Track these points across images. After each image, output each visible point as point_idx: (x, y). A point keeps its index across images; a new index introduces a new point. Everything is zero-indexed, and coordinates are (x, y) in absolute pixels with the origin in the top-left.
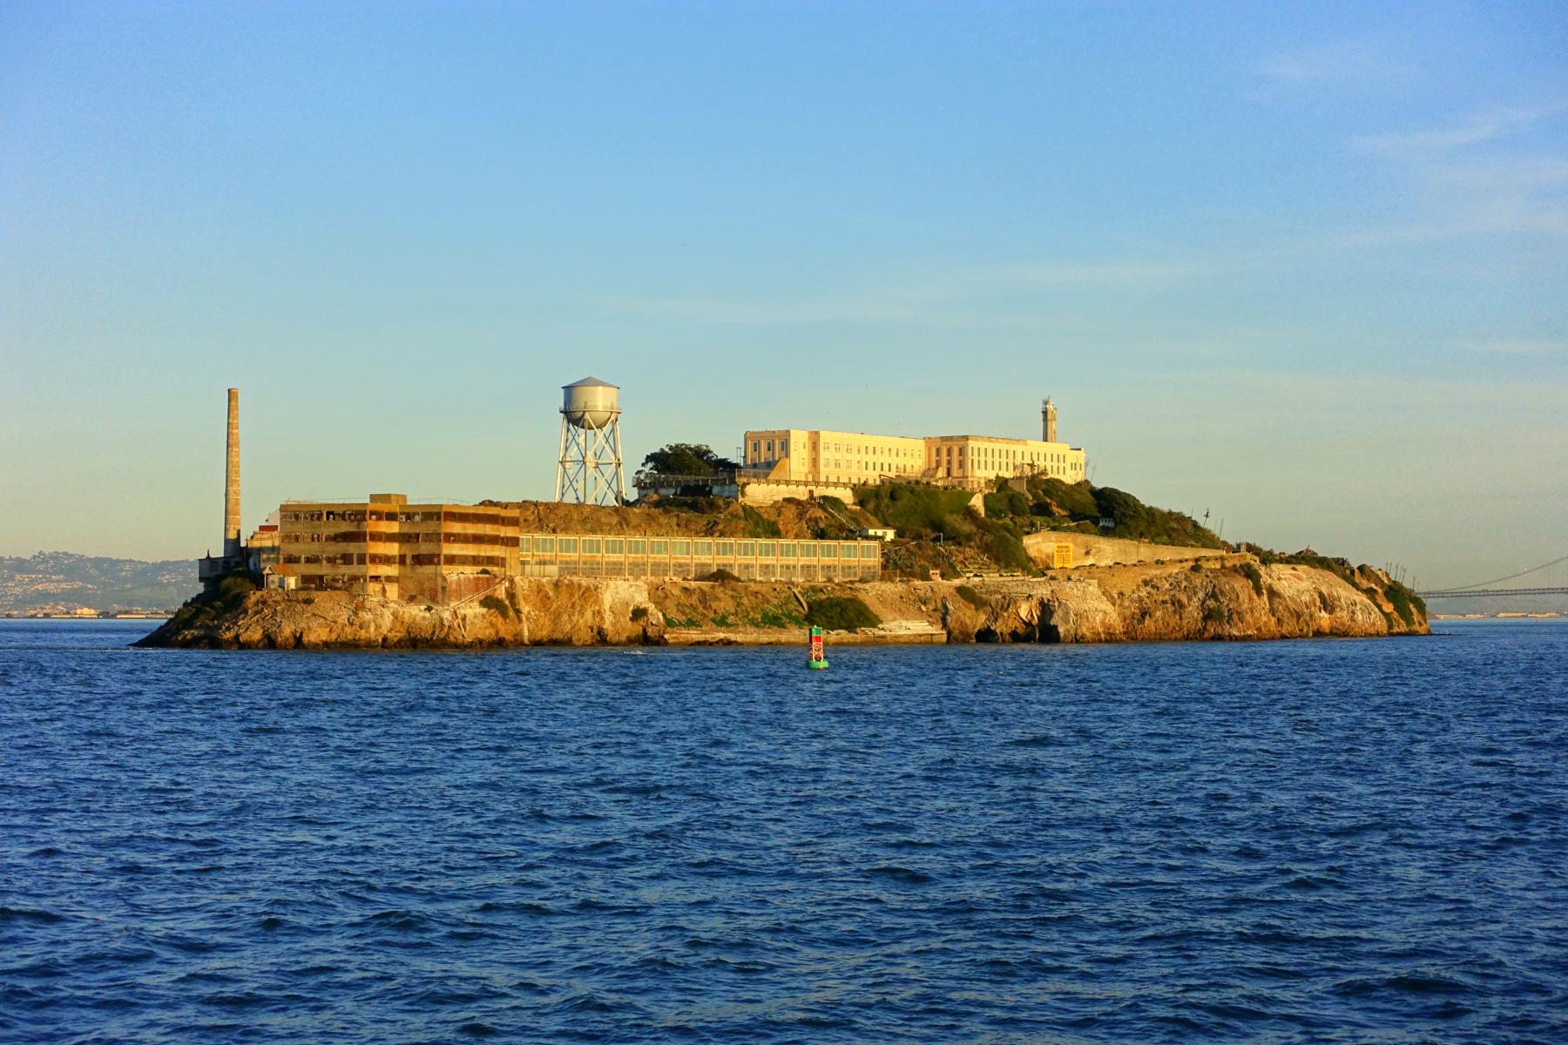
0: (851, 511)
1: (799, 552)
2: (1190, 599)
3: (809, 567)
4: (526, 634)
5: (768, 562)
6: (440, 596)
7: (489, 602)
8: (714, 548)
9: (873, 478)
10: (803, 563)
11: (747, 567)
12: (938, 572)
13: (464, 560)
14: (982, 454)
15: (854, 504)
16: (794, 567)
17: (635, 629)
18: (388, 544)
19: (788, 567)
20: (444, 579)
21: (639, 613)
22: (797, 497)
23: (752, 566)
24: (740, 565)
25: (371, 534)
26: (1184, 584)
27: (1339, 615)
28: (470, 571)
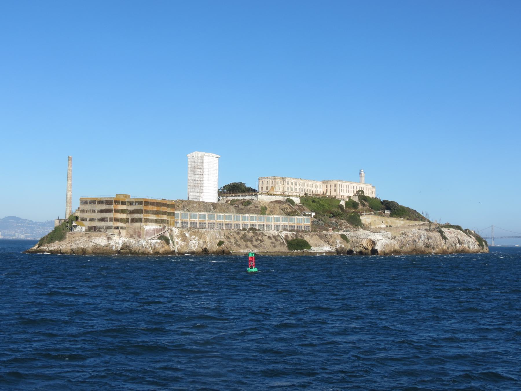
0: (298, 206)
1: (281, 220)
2: (419, 240)
5: (269, 224)
7: (162, 237)
8: (249, 218)
9: (310, 194)
10: (282, 224)
12: (332, 229)
13: (152, 221)
14: (343, 187)
15: (300, 203)
18: (121, 214)
25: (115, 210)
26: (417, 234)
27: (464, 246)
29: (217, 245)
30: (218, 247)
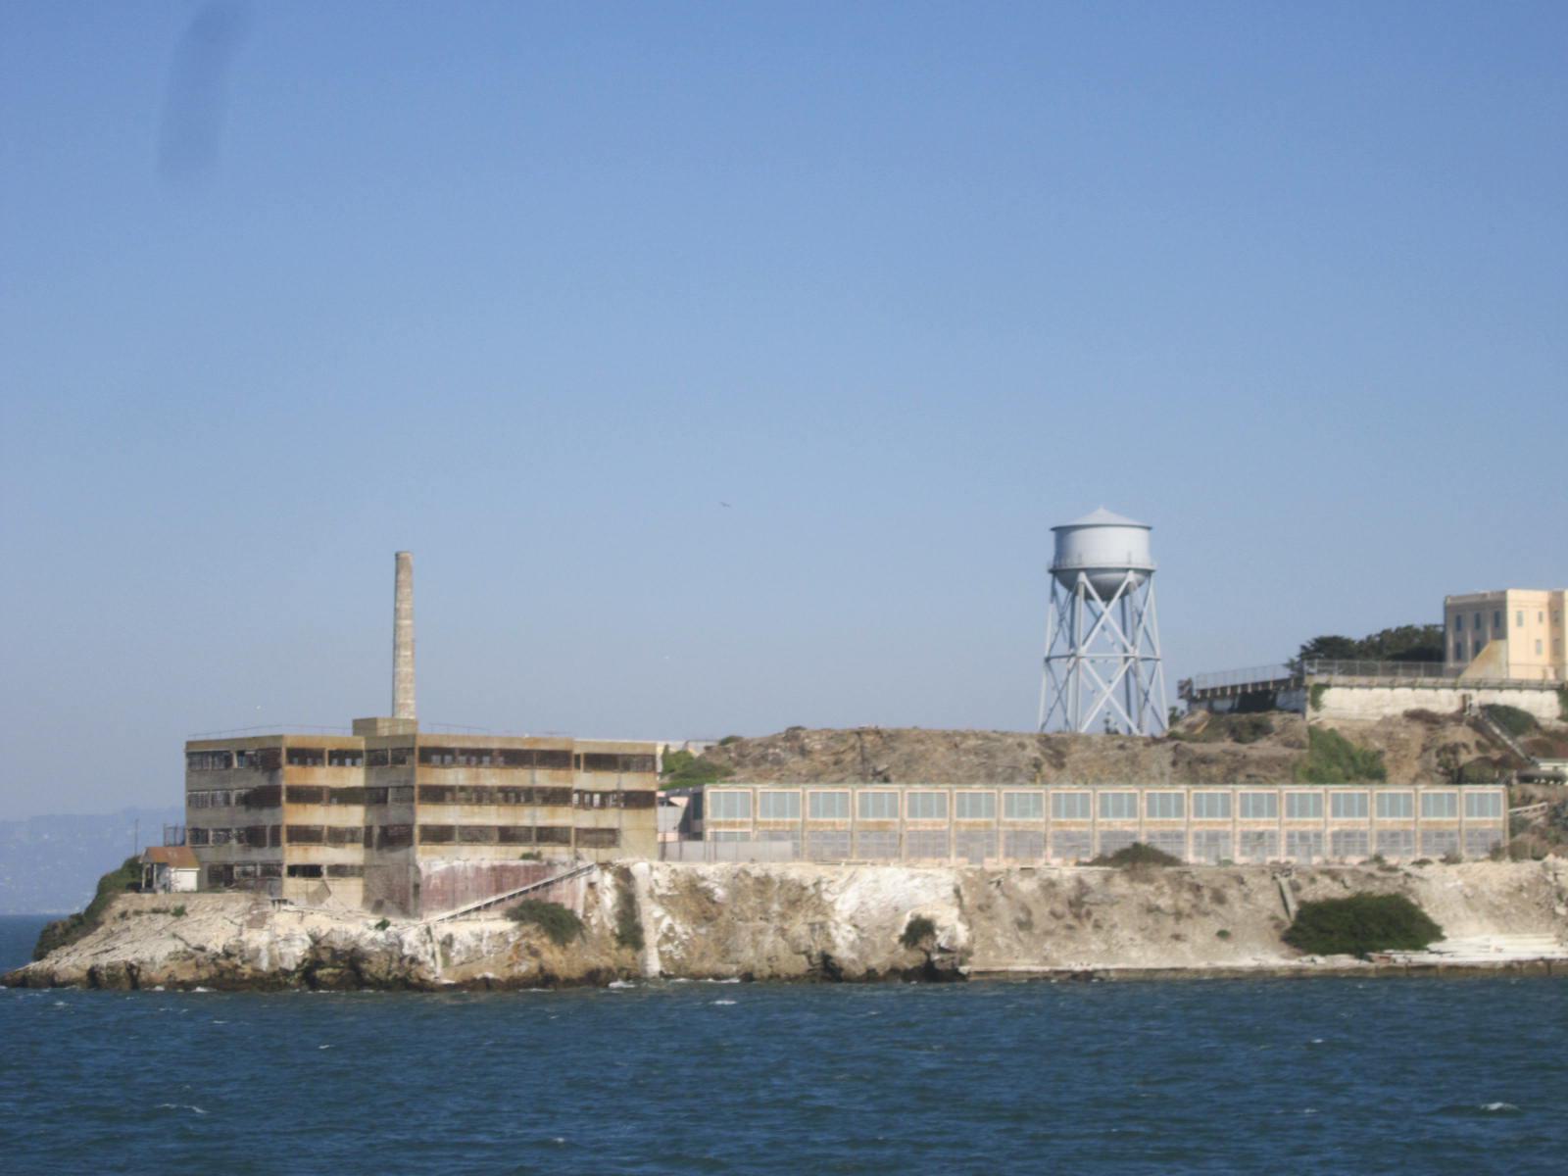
3: (1348, 835)
4: (654, 965)
5: (1261, 828)
6: (412, 900)
10: (1336, 828)
11: (1214, 838)
13: (475, 835)
16: (1318, 836)
17: (910, 959)
19: (1304, 837)
20: (418, 871)
21: (920, 930)
22: (1434, 708)
23: (1227, 836)
24: (1197, 836)
28: (489, 856)
29: (895, 940)
30: (902, 949)
